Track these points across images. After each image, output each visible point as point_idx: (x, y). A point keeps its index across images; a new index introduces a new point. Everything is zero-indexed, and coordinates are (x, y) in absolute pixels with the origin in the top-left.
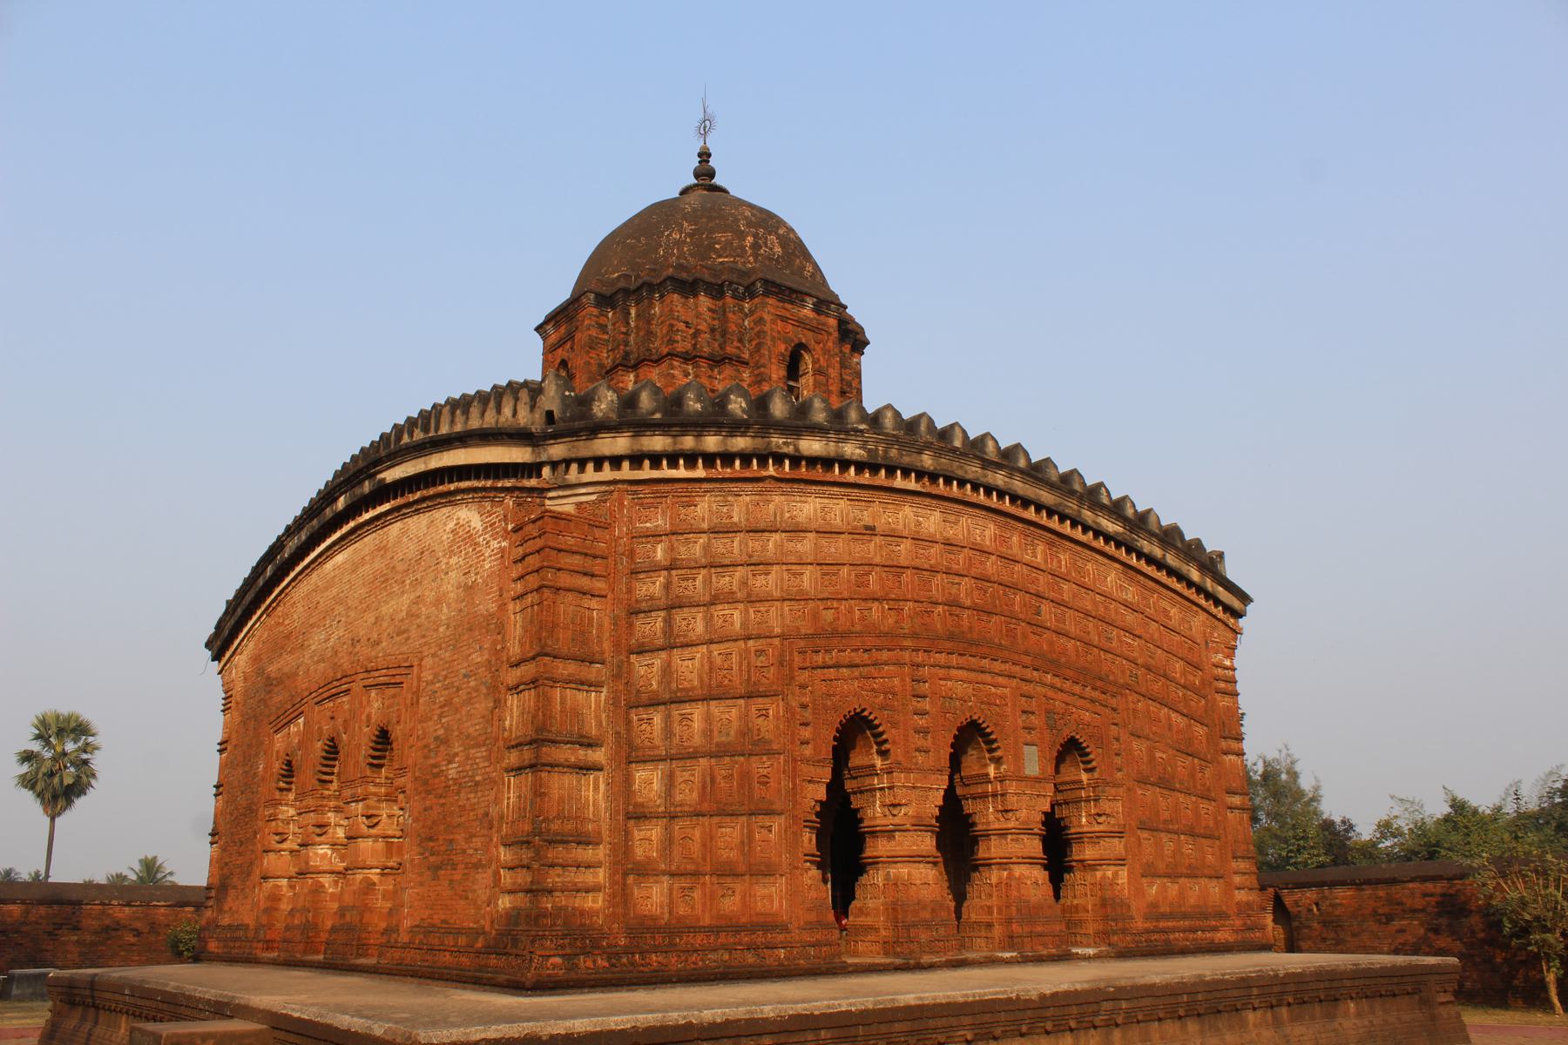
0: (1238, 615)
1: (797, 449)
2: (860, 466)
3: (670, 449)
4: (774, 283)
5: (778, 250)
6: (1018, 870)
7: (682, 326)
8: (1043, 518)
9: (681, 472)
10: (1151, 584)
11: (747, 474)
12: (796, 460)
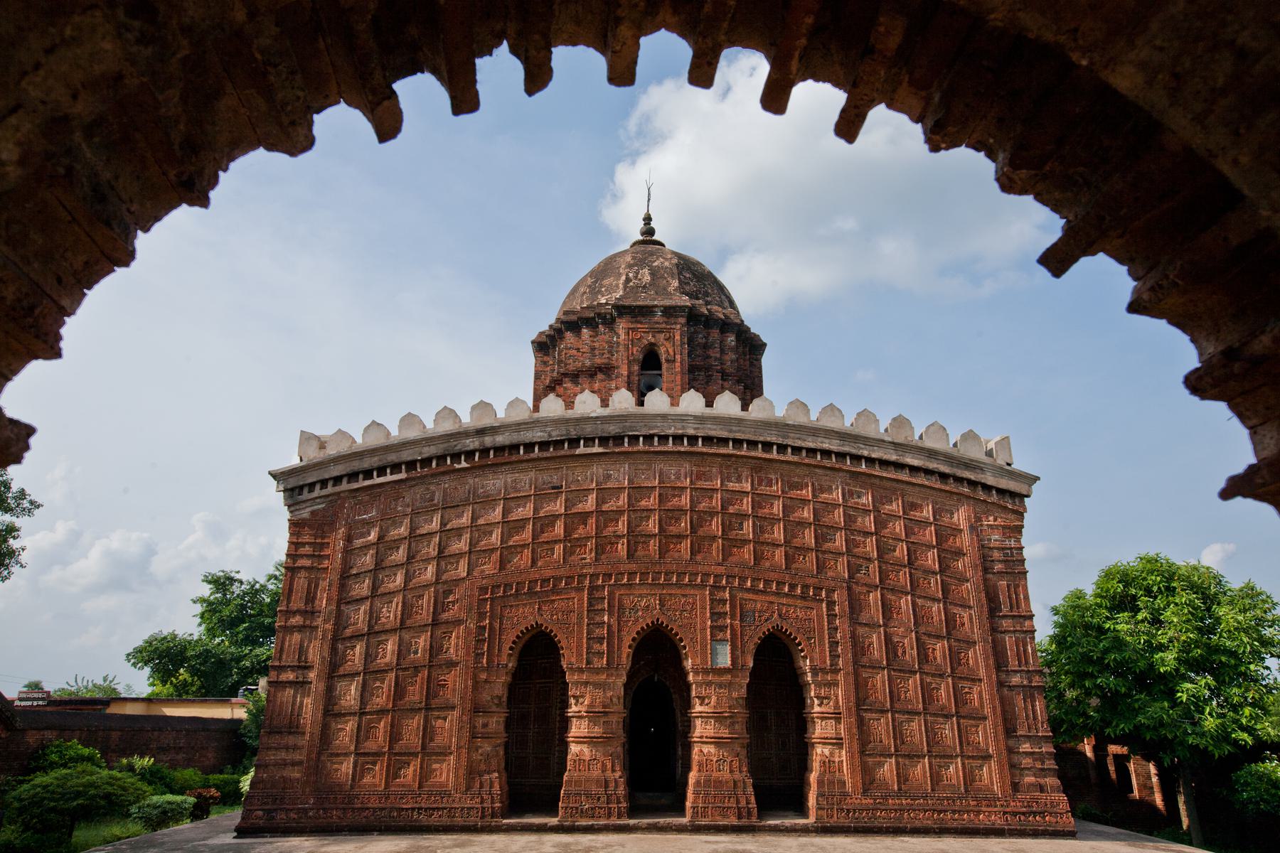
0: (1022, 497)
1: (482, 443)
2: (544, 445)
3: (376, 465)
4: (624, 307)
5: (647, 278)
7: (574, 352)
8: (744, 451)
9: (389, 478)
10: (888, 484)
11: (442, 469)
12: (484, 452)
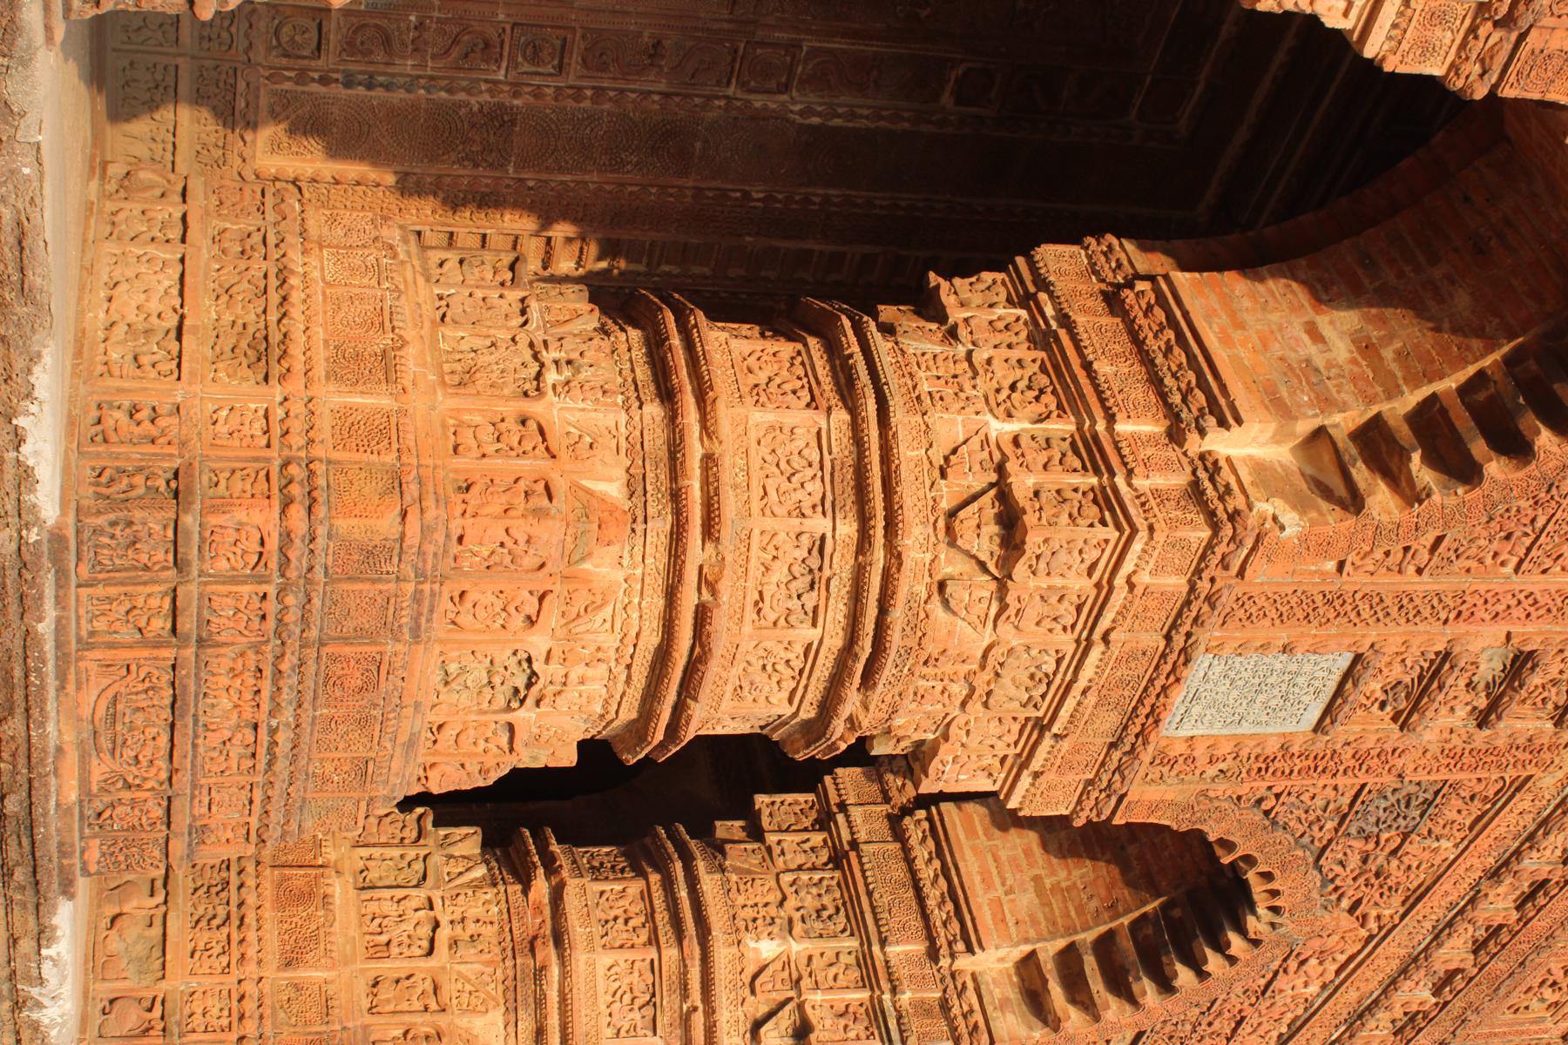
6: (624, 574)
